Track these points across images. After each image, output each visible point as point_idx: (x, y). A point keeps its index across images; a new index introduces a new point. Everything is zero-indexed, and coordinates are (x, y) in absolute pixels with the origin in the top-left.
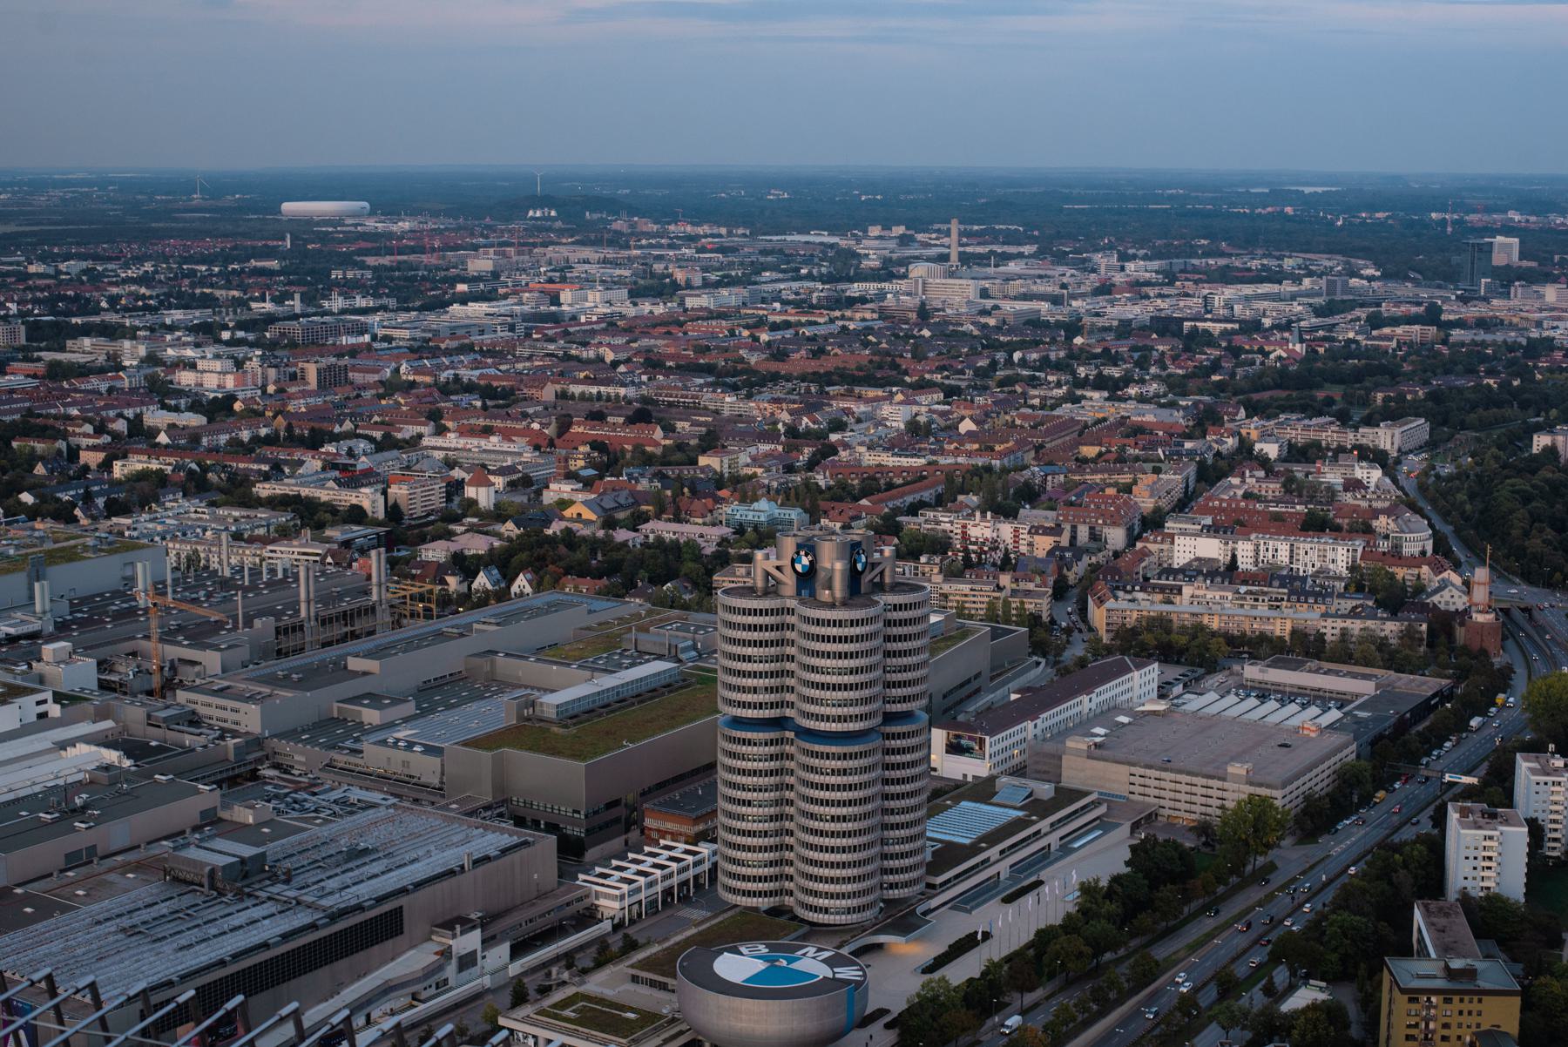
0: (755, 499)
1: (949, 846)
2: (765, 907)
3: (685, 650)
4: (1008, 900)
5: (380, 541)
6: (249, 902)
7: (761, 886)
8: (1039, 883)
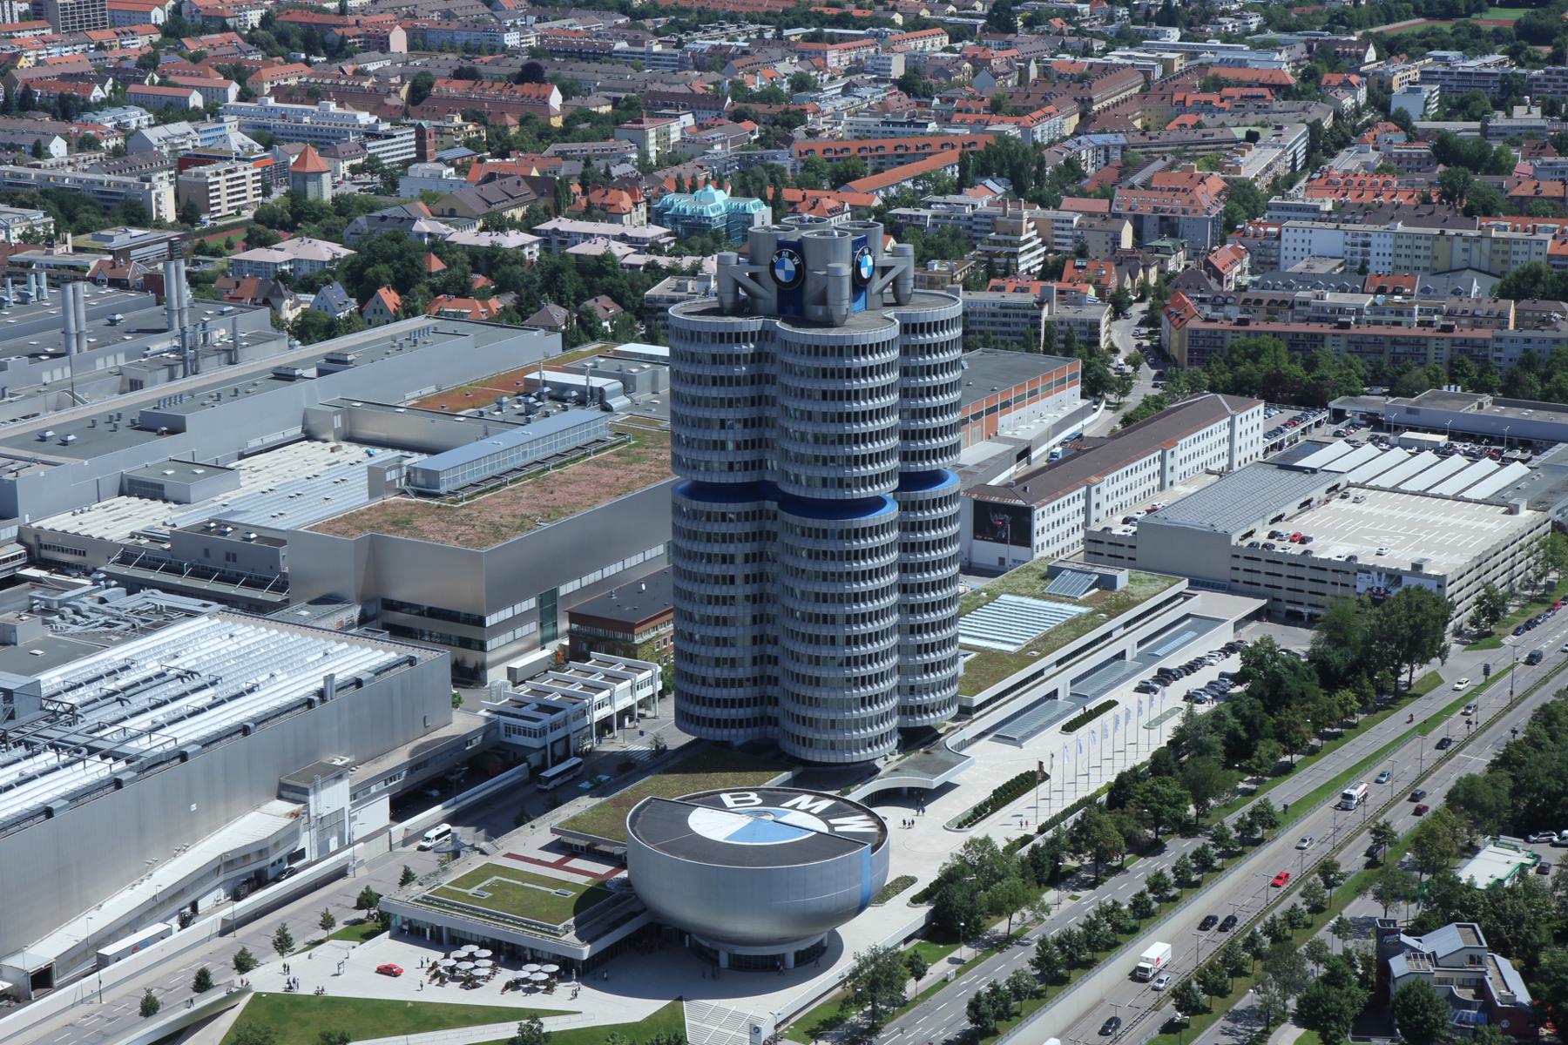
0: (693, 189)
1: (987, 656)
2: (737, 743)
3: (614, 394)
4: (1069, 728)
5: (173, 252)
6: (21, 751)
7: (734, 713)
8: (1111, 704)
